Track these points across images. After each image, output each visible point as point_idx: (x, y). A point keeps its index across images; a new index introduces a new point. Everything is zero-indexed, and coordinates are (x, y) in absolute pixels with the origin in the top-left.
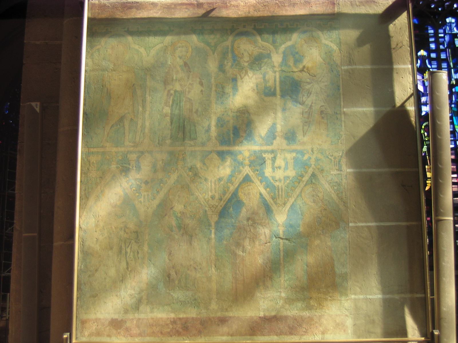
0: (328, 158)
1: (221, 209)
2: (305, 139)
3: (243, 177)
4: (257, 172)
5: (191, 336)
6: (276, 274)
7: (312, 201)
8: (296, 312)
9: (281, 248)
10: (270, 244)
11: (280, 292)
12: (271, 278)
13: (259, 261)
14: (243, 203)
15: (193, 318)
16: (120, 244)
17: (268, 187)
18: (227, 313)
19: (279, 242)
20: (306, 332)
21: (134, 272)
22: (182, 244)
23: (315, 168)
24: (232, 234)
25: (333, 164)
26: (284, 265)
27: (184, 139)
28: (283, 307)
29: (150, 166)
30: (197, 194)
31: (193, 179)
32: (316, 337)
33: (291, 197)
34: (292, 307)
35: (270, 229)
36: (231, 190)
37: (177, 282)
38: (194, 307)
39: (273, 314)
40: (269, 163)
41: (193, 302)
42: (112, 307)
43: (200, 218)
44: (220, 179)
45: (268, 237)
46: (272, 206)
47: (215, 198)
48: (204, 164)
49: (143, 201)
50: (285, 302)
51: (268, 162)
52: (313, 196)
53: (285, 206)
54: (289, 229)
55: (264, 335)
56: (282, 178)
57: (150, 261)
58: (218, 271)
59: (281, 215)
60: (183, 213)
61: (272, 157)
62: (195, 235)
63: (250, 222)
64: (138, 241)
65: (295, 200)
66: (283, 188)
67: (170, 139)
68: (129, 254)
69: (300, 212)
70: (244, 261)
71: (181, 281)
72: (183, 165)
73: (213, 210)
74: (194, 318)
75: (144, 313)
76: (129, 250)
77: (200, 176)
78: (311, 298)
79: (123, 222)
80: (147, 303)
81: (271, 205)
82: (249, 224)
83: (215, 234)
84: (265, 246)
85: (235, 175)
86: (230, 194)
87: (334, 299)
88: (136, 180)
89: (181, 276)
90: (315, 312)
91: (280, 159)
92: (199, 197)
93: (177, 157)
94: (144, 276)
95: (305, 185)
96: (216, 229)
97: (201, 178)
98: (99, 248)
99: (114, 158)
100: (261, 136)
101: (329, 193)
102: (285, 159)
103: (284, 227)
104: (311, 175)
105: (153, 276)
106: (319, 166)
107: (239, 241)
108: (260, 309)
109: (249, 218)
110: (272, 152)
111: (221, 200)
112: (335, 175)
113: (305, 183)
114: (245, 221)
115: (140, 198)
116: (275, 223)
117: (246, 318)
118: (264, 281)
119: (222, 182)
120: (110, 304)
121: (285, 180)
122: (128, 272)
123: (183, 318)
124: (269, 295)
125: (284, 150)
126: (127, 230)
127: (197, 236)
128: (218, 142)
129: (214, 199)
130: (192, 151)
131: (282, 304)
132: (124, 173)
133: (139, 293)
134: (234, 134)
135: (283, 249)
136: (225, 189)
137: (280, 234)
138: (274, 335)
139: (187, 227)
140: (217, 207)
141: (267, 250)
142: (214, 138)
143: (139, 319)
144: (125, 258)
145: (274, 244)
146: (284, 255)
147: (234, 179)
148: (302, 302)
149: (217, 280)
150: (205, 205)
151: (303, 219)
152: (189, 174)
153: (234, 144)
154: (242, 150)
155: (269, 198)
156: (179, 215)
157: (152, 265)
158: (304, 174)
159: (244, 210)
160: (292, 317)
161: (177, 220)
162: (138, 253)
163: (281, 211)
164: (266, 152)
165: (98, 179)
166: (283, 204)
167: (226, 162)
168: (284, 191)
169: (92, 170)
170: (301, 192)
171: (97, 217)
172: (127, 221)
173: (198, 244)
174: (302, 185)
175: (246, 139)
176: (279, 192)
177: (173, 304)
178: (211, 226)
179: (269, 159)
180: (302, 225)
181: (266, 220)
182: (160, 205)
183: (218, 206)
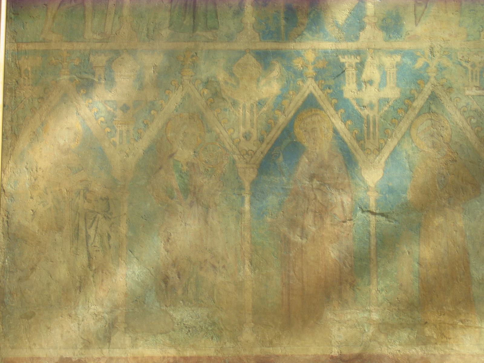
0: (461, 65)
2: (420, 30)
3: (302, 99)
4: (329, 91)
6: (362, 279)
7: (430, 144)
8: (399, 348)
9: (373, 231)
10: (352, 222)
11: (370, 311)
12: (353, 285)
13: (332, 254)
14: (303, 147)
15: (209, 358)
16: (76, 221)
18: (271, 349)
19: (368, 219)
21: (103, 272)
22: (189, 222)
23: (436, 84)
24: (281, 203)
25: (470, 76)
26: (377, 262)
27: (194, 28)
28: (374, 339)
29: (133, 77)
30: (217, 129)
33: (391, 136)
34: (391, 340)
35: (352, 196)
36: (281, 124)
37: (180, 292)
39: (356, 351)
40: (350, 73)
41: (210, 328)
42: (62, 336)
43: (224, 175)
44: (261, 103)
45: (347, 210)
46: (355, 154)
47: (251, 137)
48: (232, 74)
49: (119, 142)
50: (379, 329)
51: (350, 72)
52: (432, 136)
53: (379, 154)
54: (387, 195)
56: (375, 101)
57: (132, 252)
58: (256, 272)
60: (193, 164)
61: (357, 63)
62: (214, 206)
63: (316, 183)
64: (110, 216)
65: (399, 144)
66: (377, 122)
67: (169, 27)
68: (92, 239)
69: (407, 166)
71: (189, 289)
72: (192, 76)
73: (248, 160)
75: (119, 348)
76: (92, 232)
77: (224, 96)
78: (426, 323)
79: (81, 181)
80: (126, 330)
81: (354, 152)
82: (314, 186)
83: (251, 203)
84: (342, 226)
85: (289, 95)
86: (278, 129)
87: (468, 326)
88: (105, 102)
89: (189, 280)
90: (433, 349)
91: (372, 67)
92: (221, 135)
93: (182, 61)
94: (121, 279)
95: (418, 116)
96: (253, 195)
97: (226, 101)
98: (36, 228)
99: (66, 62)
100: (337, 24)
101: (462, 130)
102: (381, 67)
103: (377, 192)
104: (429, 96)
105: (137, 279)
106: (444, 81)
108: (333, 343)
109: (314, 174)
110: (358, 53)
112: (473, 96)
113: (417, 111)
114: (307, 180)
115: (113, 137)
116: (362, 185)
117: (307, 357)
118: (340, 292)
119: (265, 109)
120: (57, 330)
121: (380, 106)
122: (91, 273)
123: (191, 357)
124: (349, 317)
125: (380, 49)
126: (88, 195)
127: (218, 207)
128: (257, 34)
129: (250, 139)
130: (209, 51)
131: (373, 333)
132: (84, 91)
133: (112, 312)
134: (286, 19)
135: (376, 232)
137: (371, 205)
139: (199, 191)
140: (254, 154)
141: (345, 235)
142: (249, 27)
143: (111, 358)
144: (86, 246)
145: (360, 222)
146: (377, 243)
147: (286, 102)
148: (409, 330)
149: (254, 288)
150: (233, 150)
151: (413, 177)
152: (204, 93)
153: (288, 37)
154: (302, 50)
156: (185, 168)
157: (135, 260)
158: (416, 95)
159: (305, 160)
160: (390, 357)
161: (182, 177)
162: (109, 237)
163: (373, 162)
164: (346, 53)
165: (36, 100)
166: (377, 149)
167: (271, 71)
169: (25, 85)
170: (410, 129)
171: (34, 170)
172: (89, 179)
173: (219, 222)
174: (412, 114)
175: (309, 29)
176: (369, 127)
177: (173, 332)
178: (244, 189)
179: (351, 66)
180: (411, 189)
181: (345, 179)
182: (149, 150)
183: (256, 152)
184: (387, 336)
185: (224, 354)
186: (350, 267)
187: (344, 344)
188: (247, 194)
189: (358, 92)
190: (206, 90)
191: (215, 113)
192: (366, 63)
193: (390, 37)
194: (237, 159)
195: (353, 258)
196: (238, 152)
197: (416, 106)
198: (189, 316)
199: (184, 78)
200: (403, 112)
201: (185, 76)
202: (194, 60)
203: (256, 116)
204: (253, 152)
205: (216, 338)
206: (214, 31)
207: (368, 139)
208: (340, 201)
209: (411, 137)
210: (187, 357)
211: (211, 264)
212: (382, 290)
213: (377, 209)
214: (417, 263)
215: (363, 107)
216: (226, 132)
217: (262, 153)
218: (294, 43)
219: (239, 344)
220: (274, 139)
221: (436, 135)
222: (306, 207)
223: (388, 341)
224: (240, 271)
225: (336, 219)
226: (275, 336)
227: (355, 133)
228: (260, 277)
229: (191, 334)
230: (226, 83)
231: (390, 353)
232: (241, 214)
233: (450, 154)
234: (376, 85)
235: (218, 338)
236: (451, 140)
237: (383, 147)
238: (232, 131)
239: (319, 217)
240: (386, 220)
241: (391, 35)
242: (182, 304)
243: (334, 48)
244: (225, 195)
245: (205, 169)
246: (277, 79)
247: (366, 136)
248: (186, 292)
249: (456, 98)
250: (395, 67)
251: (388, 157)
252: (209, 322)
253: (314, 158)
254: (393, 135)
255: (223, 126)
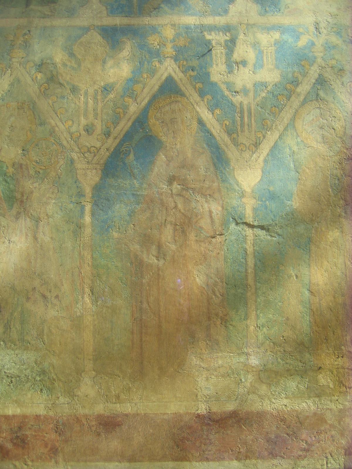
1: (109, 157)
3: (159, 83)
4: (192, 73)
5: (32, 461)
6: (237, 311)
7: (320, 139)
8: (285, 401)
9: (250, 250)
12: (225, 321)
13: (197, 280)
14: (160, 142)
15: (37, 417)
17: (217, 106)
18: (118, 405)
20: (307, 450)
22: (14, 239)
23: (324, 65)
24: (132, 214)
26: (256, 289)
28: (253, 390)
31: (46, 89)
32: (332, 461)
33: (271, 129)
34: (275, 391)
35: (223, 204)
38: (41, 390)
39: (230, 407)
40: (219, 52)
41: (38, 378)
43: (59, 178)
44: (107, 89)
45: (217, 221)
46: (226, 150)
48: (72, 55)
50: (260, 378)
51: (218, 51)
52: (322, 128)
55: (207, 460)
56: (250, 86)
58: (98, 304)
59: (249, 171)
60: (21, 166)
61: (226, 41)
65: (280, 137)
66: (253, 111)
69: (292, 166)
70: (160, 280)
73: (90, 159)
74: (40, 416)
77: (61, 81)
78: (320, 368)
81: (224, 147)
82: (174, 192)
83: (93, 214)
84: (210, 243)
85: (142, 79)
86: (128, 121)
89: (12, 314)
90: (329, 402)
92: (57, 129)
95: (304, 103)
96: (95, 204)
103: (255, 198)
104: (316, 80)
106: (334, 62)
107: (150, 230)
108: (199, 397)
110: (227, 29)
111: (109, 135)
113: (302, 98)
114: (164, 184)
117: (166, 417)
118: (208, 328)
119: (112, 96)
121: (255, 91)
123: (14, 416)
125: (254, 25)
128: (104, 8)
130: (45, 28)
131: (251, 382)
135: (254, 250)
136: (118, 110)
137: (247, 216)
138: (232, 460)
141: (214, 254)
145: (233, 238)
146: (255, 265)
147: (138, 87)
148: (298, 378)
149: (95, 325)
151: (299, 179)
152: (37, 77)
153: (142, 11)
155: (220, 131)
156: (11, 170)
158: (300, 78)
159: (162, 157)
160: (274, 414)
161: (6, 182)
163: (249, 161)
164: (212, 28)
166: (253, 144)
167: (121, 50)
168: (255, 116)
170: (293, 119)
174: (296, 102)
176: (244, 117)
178: (84, 196)
180: (298, 195)
181: (213, 182)
183: (100, 148)
184: (270, 386)
185: (56, 412)
186: (221, 297)
187: (213, 399)
188: (87, 202)
189: (229, 75)
190: (40, 74)
191: (50, 102)
192: (237, 40)
193: (266, 11)
194: (76, 158)
195: (224, 284)
196: (77, 149)
197: (301, 92)
198: (11, 361)
199: (14, 60)
200: (285, 99)
201: (14, 58)
202: (26, 39)
203: (100, 105)
204: (97, 148)
205: (47, 391)
206: (52, 5)
207: (243, 131)
208: (208, 210)
209: (296, 130)
210: (9, 416)
211: (40, 293)
212: (263, 326)
213: (255, 221)
214: (308, 290)
215: (235, 92)
216: (64, 125)
217: (107, 149)
218: (149, 18)
219: (75, 400)
220: (123, 133)
221: (326, 128)
222: (164, 218)
223: (271, 393)
224: (77, 303)
225: (202, 233)
226: (123, 389)
227: (226, 124)
228: (104, 311)
229: (13, 386)
230: (65, 65)
231: (274, 409)
232: (80, 228)
233: (345, 151)
234: (250, 66)
235: (48, 391)
236: (345, 133)
237: (261, 142)
238: (70, 123)
239: (180, 231)
240: (266, 234)
241: (267, 9)
242: (2, 345)
243: (198, 23)
244: (60, 204)
245: (36, 172)
246: (127, 60)
247: (239, 128)
248: (9, 330)
249: (349, 82)
250: (273, 45)
251: (268, 155)
252: (38, 370)
253: (174, 155)
254: (274, 127)
255: (60, 118)
